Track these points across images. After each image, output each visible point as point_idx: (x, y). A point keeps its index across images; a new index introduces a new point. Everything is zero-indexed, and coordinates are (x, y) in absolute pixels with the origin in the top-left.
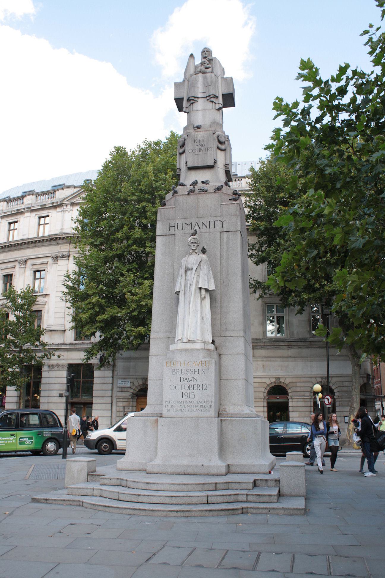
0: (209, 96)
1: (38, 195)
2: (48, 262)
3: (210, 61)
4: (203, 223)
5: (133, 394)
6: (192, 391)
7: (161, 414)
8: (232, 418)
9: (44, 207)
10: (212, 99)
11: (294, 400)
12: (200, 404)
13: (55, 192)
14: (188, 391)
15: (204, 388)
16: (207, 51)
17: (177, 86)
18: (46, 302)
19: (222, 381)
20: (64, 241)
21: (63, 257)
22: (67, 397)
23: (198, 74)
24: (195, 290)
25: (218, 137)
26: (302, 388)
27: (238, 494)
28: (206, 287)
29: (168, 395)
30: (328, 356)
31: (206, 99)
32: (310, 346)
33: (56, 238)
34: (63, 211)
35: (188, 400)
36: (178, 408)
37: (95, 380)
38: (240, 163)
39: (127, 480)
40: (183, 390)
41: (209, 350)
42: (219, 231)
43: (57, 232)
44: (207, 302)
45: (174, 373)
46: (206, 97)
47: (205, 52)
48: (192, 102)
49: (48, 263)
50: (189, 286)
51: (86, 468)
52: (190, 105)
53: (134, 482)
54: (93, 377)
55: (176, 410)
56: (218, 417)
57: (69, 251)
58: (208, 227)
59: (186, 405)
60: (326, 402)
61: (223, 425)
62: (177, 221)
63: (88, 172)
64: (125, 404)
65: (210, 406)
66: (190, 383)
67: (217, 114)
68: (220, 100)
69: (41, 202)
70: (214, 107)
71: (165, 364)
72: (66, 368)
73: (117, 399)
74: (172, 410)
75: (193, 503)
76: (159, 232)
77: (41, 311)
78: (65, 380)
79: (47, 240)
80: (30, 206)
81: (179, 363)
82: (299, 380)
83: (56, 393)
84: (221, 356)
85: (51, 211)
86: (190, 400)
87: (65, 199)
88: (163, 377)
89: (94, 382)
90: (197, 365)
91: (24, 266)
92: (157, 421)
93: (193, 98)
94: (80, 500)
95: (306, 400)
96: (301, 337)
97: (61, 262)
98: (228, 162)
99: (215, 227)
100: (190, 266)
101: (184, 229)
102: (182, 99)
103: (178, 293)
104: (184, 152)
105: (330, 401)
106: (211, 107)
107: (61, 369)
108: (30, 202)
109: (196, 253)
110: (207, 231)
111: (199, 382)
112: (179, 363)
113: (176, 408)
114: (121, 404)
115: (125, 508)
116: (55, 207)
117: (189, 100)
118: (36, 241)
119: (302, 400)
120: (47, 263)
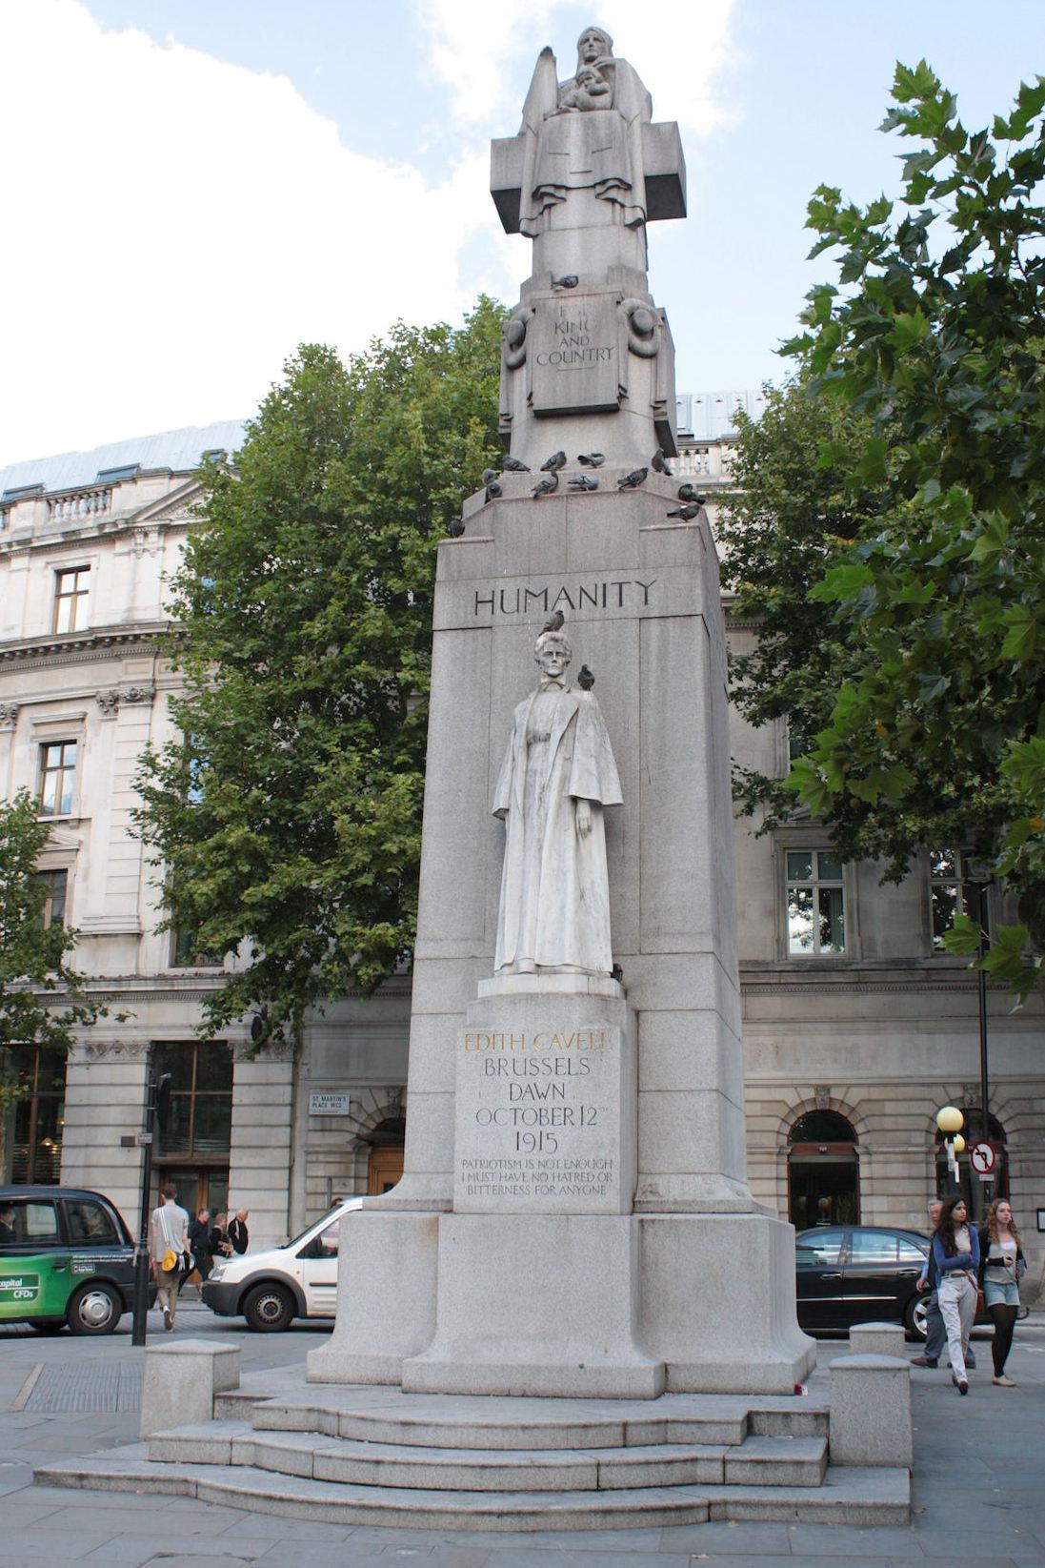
0: (604, 182)
1: (53, 500)
2: (85, 714)
3: (607, 69)
4: (582, 589)
5: (359, 1137)
6: (549, 1128)
7: (450, 1201)
8: (676, 1216)
9: (72, 540)
10: (613, 194)
11: (875, 1158)
12: (573, 1170)
13: (107, 490)
14: (537, 1128)
15: (587, 1118)
16: (595, 39)
17: (501, 149)
18: (81, 843)
19: (645, 1097)
20: (139, 647)
21: (134, 699)
22: (148, 1147)
23: (568, 111)
24: (559, 806)
25: (631, 315)
26: (900, 1120)
27: (694, 1460)
28: (594, 796)
29: (472, 1141)
30: (983, 1017)
31: (592, 193)
32: (925, 984)
33: (113, 639)
34: (135, 551)
35: (537, 1156)
36: (504, 1184)
37: (238, 1095)
38: (703, 399)
39: (338, 1415)
40: (520, 1127)
41: (604, 999)
42: (637, 615)
43: (117, 620)
44: (597, 841)
45: (490, 1071)
46: (594, 186)
47: (591, 41)
48: (547, 201)
49: (88, 718)
50: (538, 790)
51: (210, 1375)
52: (542, 213)
53: (363, 1419)
54: (229, 1084)
55: (496, 1190)
56: (633, 1212)
57: (154, 681)
58: (600, 602)
59: (529, 1172)
60: (978, 1163)
61: (649, 1239)
62: (501, 584)
63: (214, 427)
64: (332, 1170)
65: (607, 1177)
66: (541, 1103)
67: (629, 241)
68: (639, 195)
69: (63, 524)
70: (618, 219)
71: (461, 1043)
72: (143, 1056)
73: (307, 1153)
74: (484, 1189)
75: (552, 1486)
76: (441, 617)
77: (65, 871)
78: (139, 1095)
79: (83, 644)
80: (27, 535)
81: (508, 1038)
82: (891, 1092)
83: (111, 1136)
84: (642, 1016)
85: (94, 551)
86: (543, 1156)
87: (139, 513)
88: (453, 1085)
89: (235, 1101)
90: (563, 1044)
91: (9, 728)
92: (434, 1225)
93: (551, 190)
94: (189, 1478)
95: (912, 1157)
96: (897, 955)
97: (129, 715)
98: (663, 396)
99: (621, 604)
100: (541, 728)
101: (522, 609)
102: (517, 192)
103: (502, 814)
104: (522, 362)
105: (990, 1162)
106: (608, 218)
107: (127, 1057)
108: (28, 523)
109: (561, 686)
110: (597, 616)
111: (569, 1101)
112: (508, 1038)
113: (495, 1182)
114: (320, 1171)
115: (334, 1505)
116: (108, 537)
117: (537, 195)
118: (47, 649)
119: (900, 1157)
120: (83, 720)
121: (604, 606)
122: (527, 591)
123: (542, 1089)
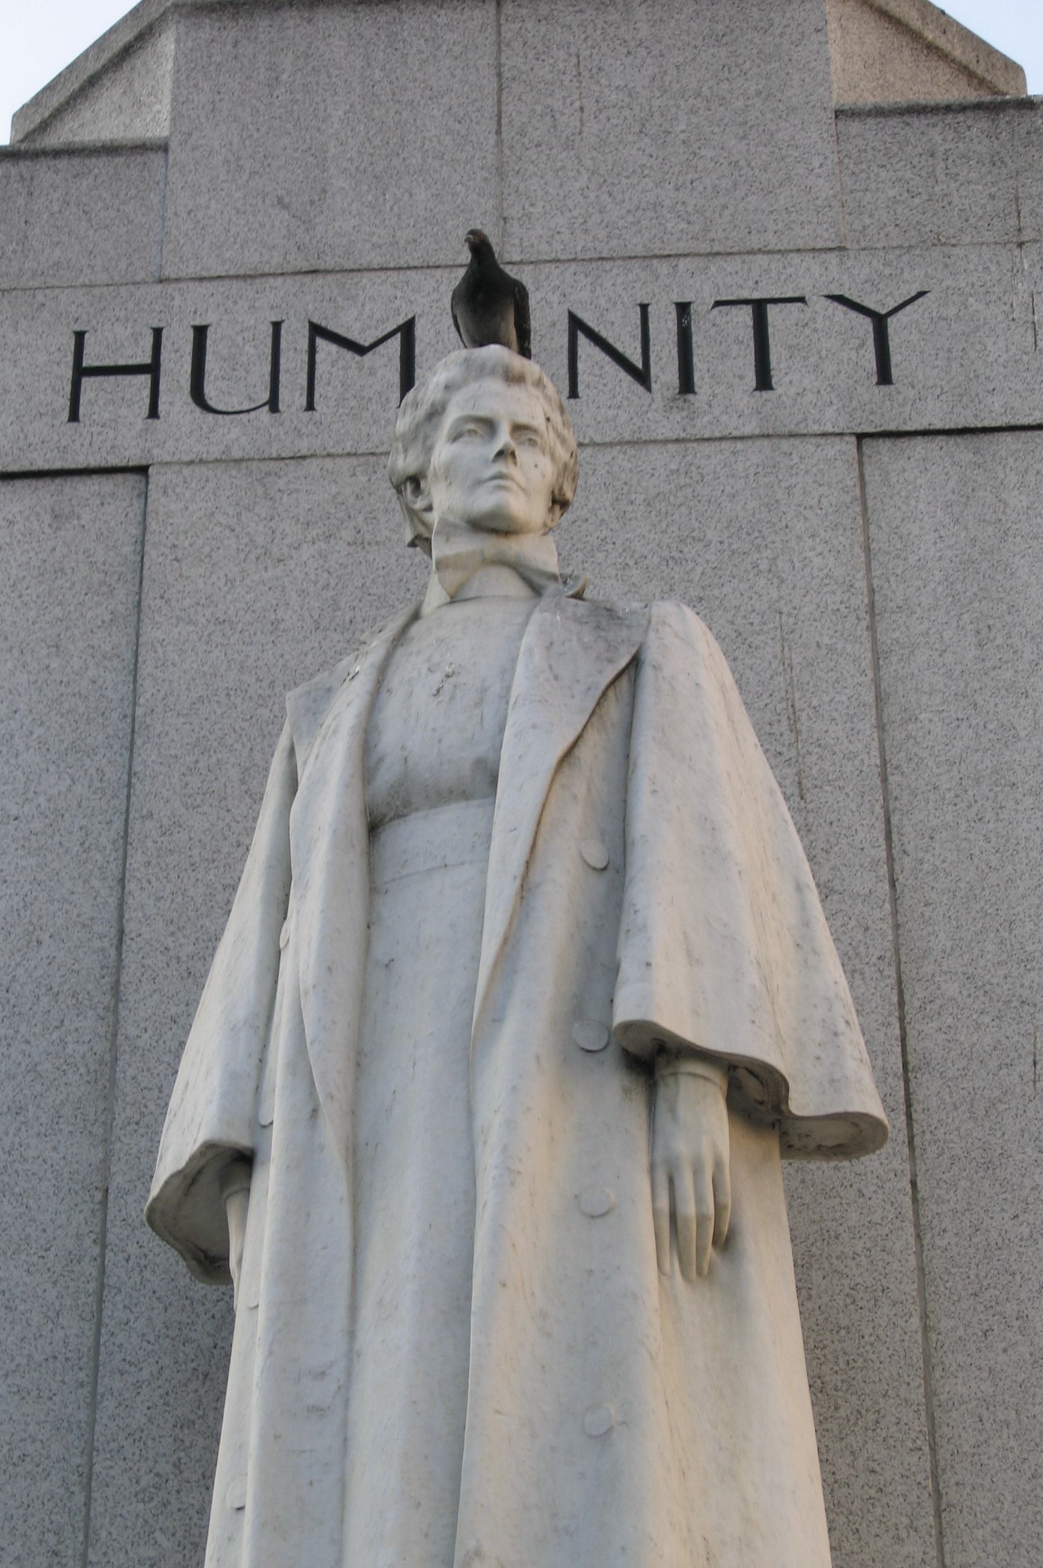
4: (576, 325)
101: (292, 394)
121: (687, 385)
122: (317, 331)
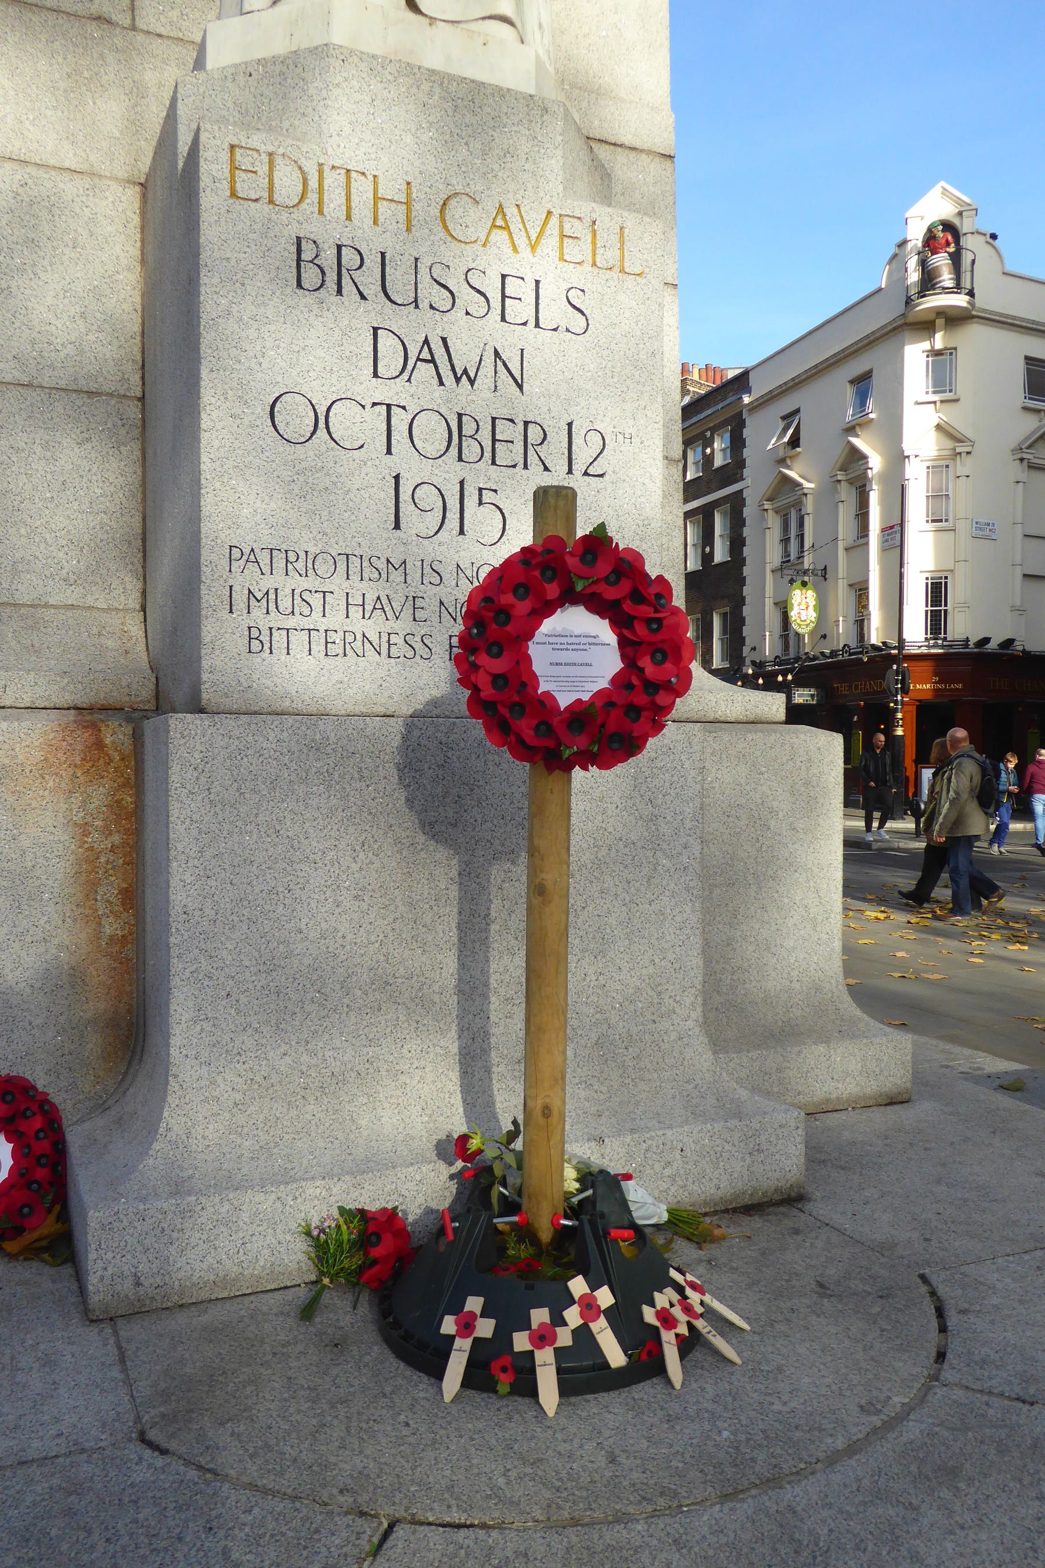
6: (480, 475)
45: (311, 277)
74: (299, 640)
113: (335, 619)
123: (465, 357)
